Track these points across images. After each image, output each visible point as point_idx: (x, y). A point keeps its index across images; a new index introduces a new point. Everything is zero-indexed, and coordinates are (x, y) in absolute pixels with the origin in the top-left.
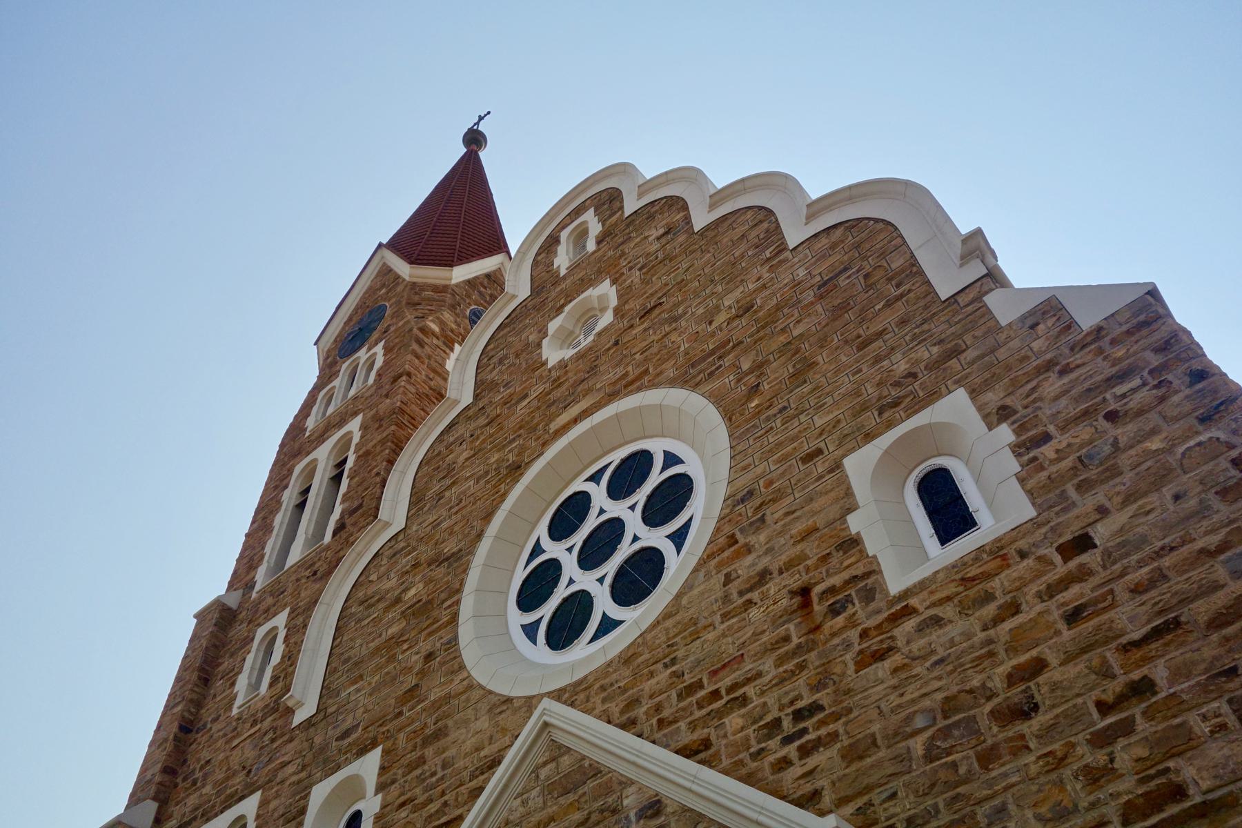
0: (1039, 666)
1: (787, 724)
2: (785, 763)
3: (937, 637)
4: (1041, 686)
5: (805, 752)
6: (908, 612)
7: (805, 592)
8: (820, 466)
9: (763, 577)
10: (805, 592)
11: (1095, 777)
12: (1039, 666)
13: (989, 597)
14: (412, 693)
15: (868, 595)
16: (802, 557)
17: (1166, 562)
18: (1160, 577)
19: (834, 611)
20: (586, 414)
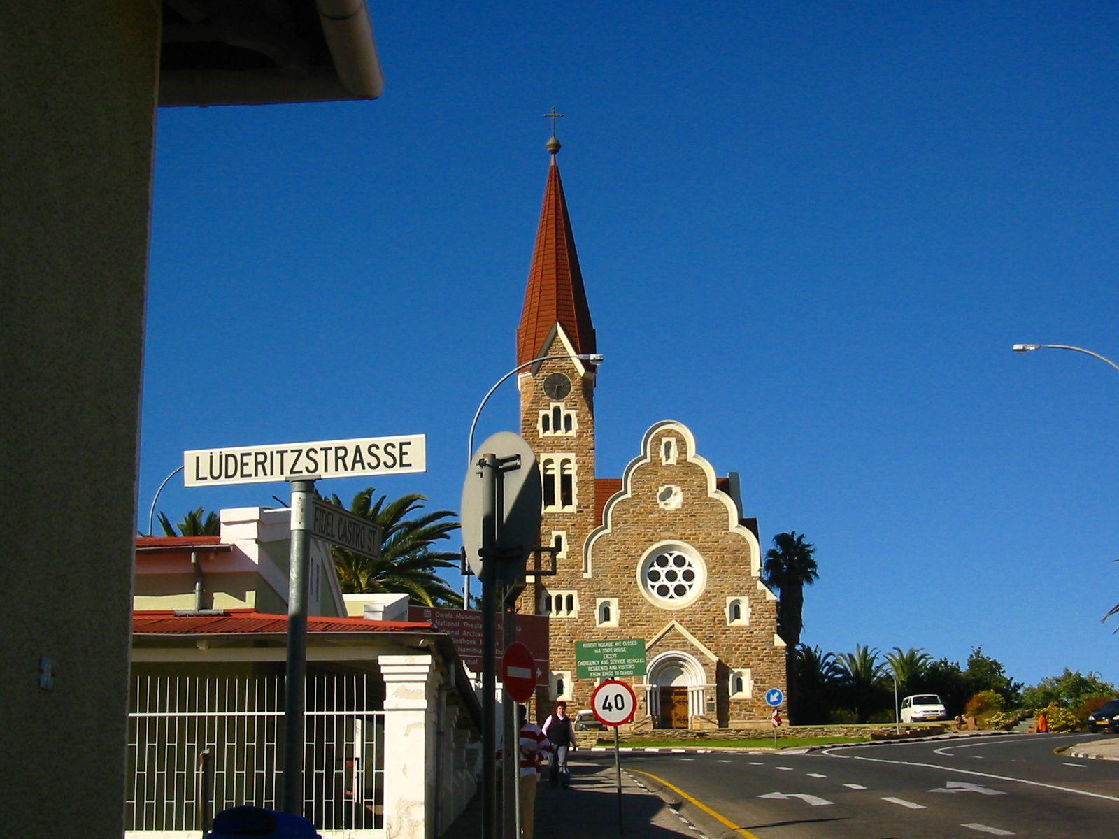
0: (742, 645)
1: (708, 637)
2: (706, 642)
3: (732, 635)
4: (741, 648)
5: (710, 642)
6: (729, 630)
7: (715, 618)
8: (723, 595)
9: (709, 611)
10: (715, 618)
11: (743, 660)
12: (742, 645)
13: (739, 633)
14: (626, 589)
15: (725, 624)
16: (716, 611)
17: (759, 640)
18: (757, 642)
19: (719, 624)
20: (674, 539)
